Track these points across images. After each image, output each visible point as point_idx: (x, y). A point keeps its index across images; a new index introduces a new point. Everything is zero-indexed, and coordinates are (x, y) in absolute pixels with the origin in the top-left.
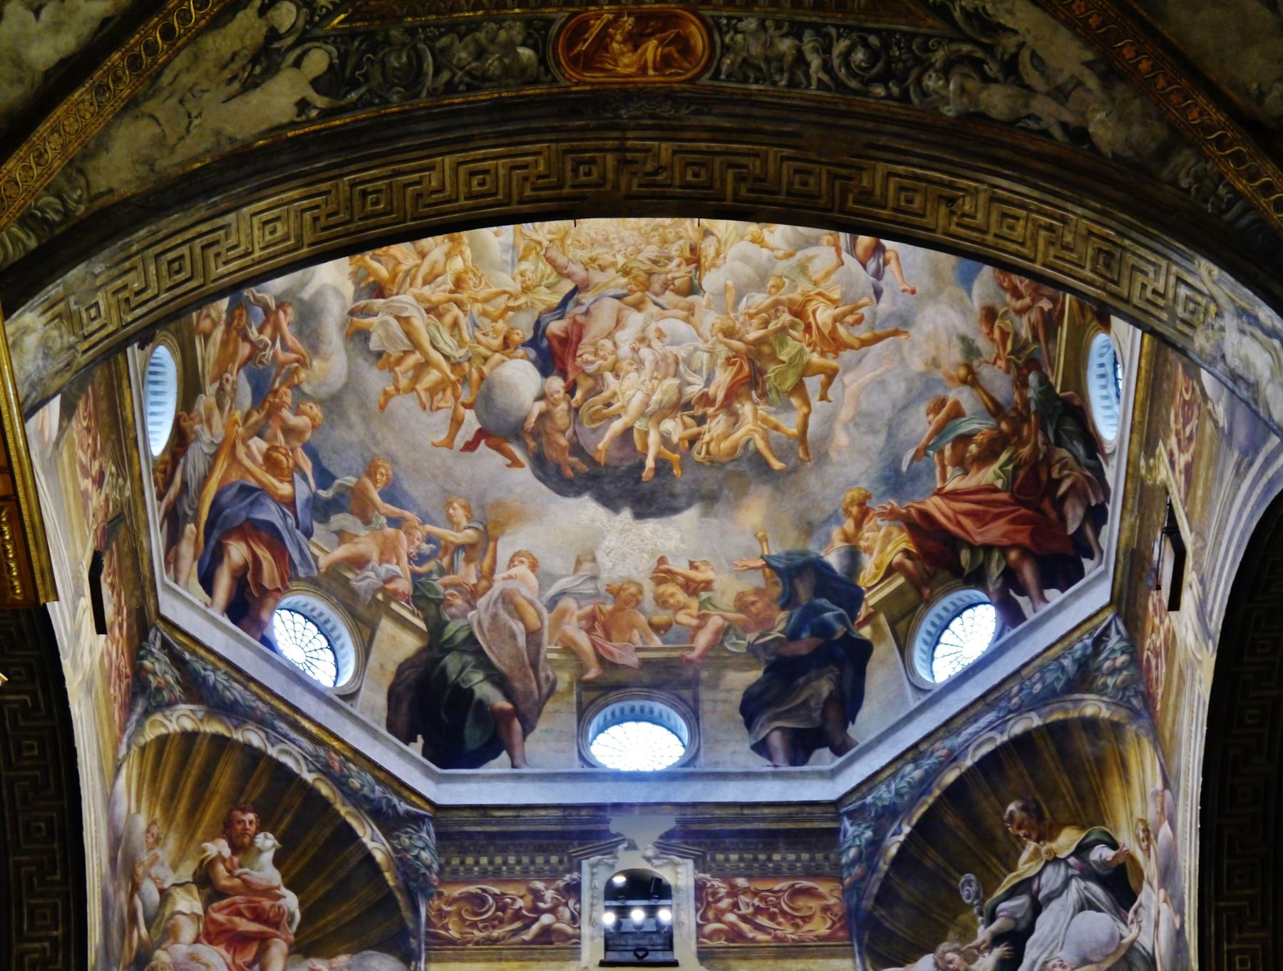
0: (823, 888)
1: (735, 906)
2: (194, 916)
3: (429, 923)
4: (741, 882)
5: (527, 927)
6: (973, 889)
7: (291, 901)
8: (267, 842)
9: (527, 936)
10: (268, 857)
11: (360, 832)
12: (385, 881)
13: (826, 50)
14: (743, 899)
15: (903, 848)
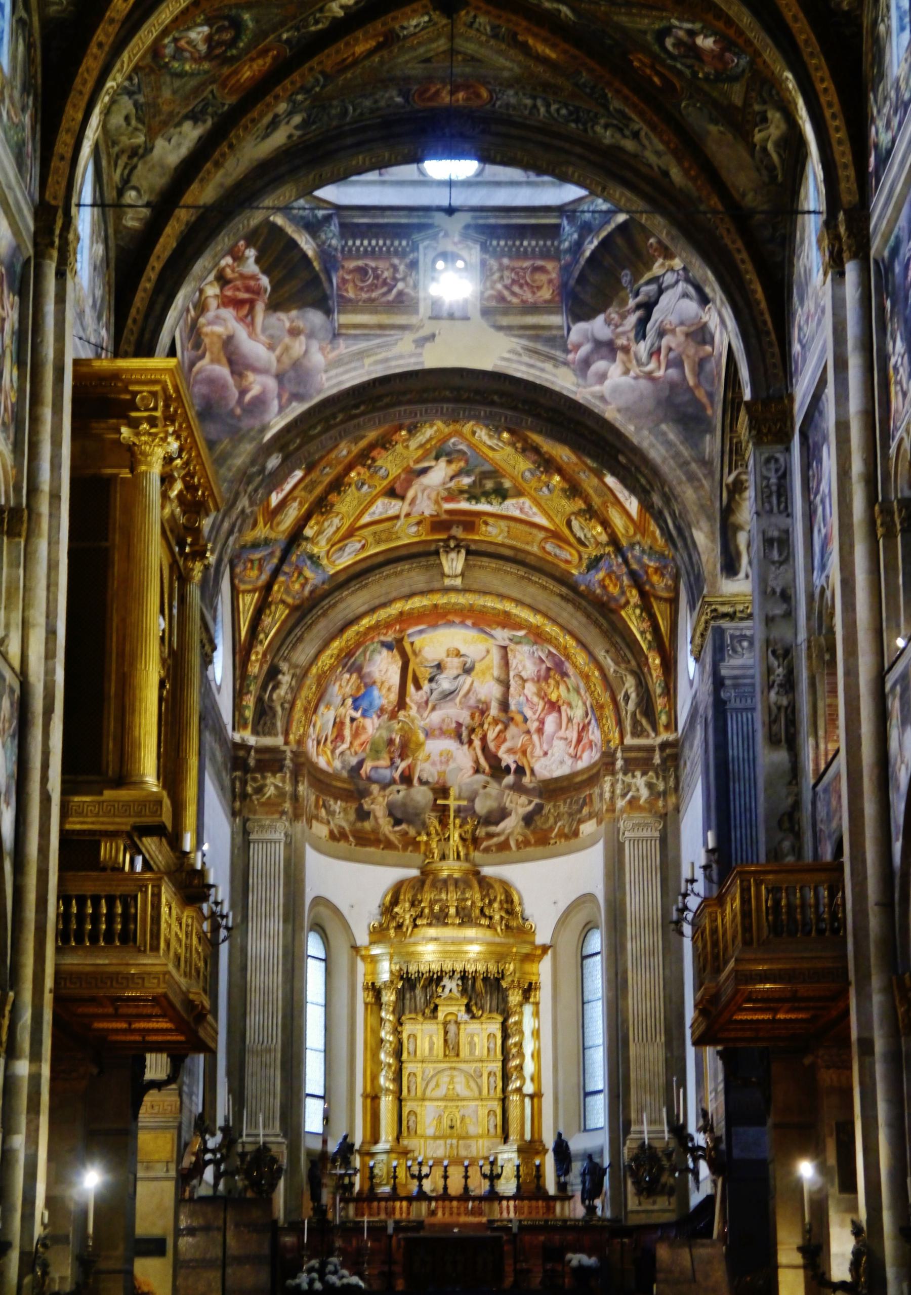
0: (550, 266)
1: (502, 278)
2: (216, 296)
3: (339, 288)
4: (506, 261)
5: (390, 291)
6: (629, 278)
7: (265, 281)
8: (251, 253)
9: (391, 297)
10: (252, 260)
11: (299, 242)
12: (314, 268)
13: (548, 106)
14: (506, 273)
15: (593, 253)
